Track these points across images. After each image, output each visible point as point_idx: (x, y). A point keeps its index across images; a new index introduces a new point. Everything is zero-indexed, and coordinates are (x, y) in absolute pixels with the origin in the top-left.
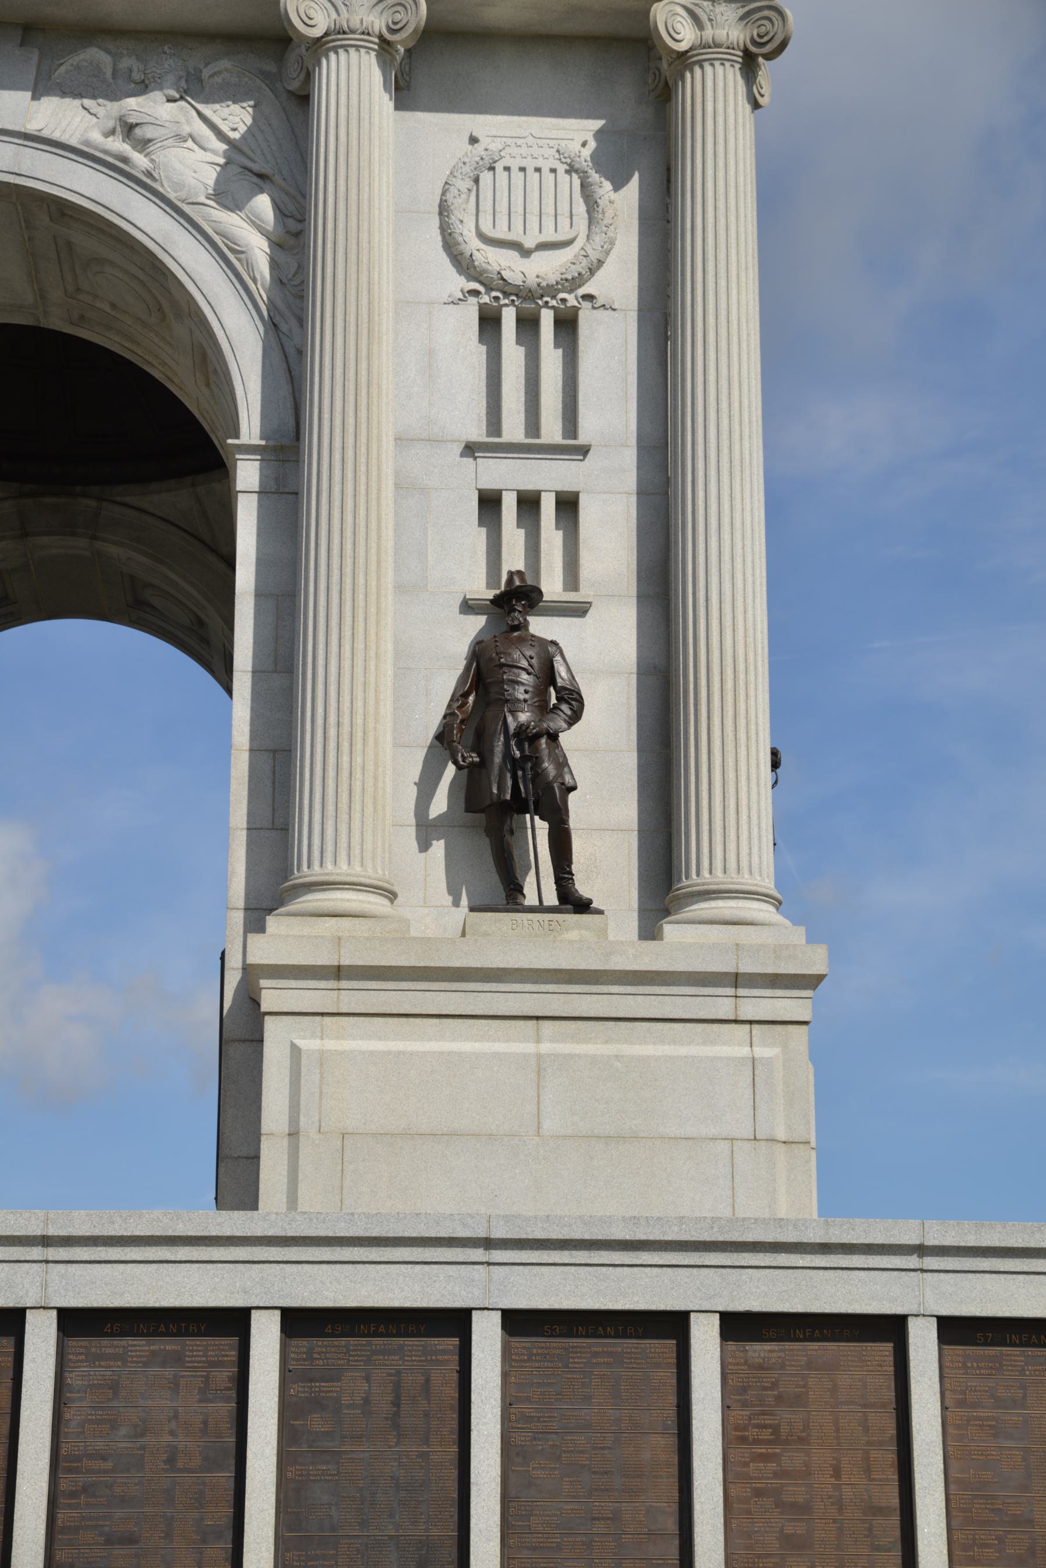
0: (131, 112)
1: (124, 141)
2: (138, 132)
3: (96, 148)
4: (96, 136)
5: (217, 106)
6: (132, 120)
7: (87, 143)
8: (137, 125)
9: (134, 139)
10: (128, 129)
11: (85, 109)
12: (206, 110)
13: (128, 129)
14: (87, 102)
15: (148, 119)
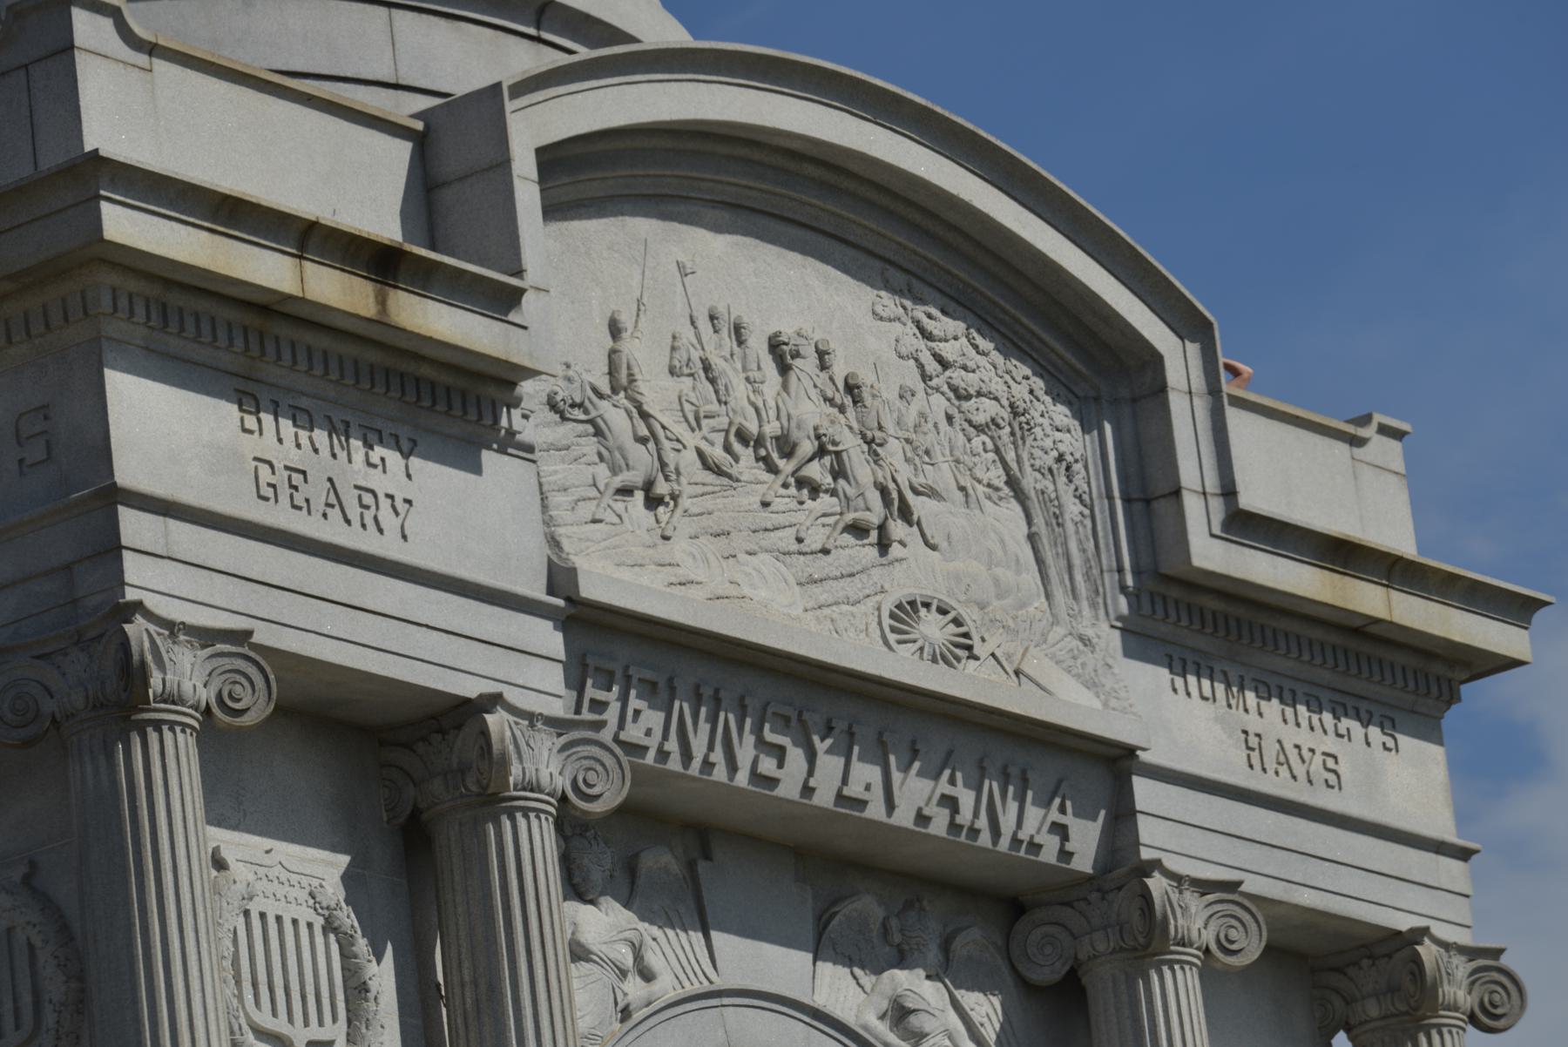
0: (907, 992)
1: (891, 1030)
2: (913, 1019)
3: (876, 1038)
4: (872, 1019)
5: (963, 992)
6: (910, 1005)
7: (866, 1028)
8: (914, 1011)
9: (906, 1029)
10: (899, 1014)
11: (855, 977)
12: (959, 994)
13: (899, 1014)
14: (857, 971)
15: (926, 1008)
